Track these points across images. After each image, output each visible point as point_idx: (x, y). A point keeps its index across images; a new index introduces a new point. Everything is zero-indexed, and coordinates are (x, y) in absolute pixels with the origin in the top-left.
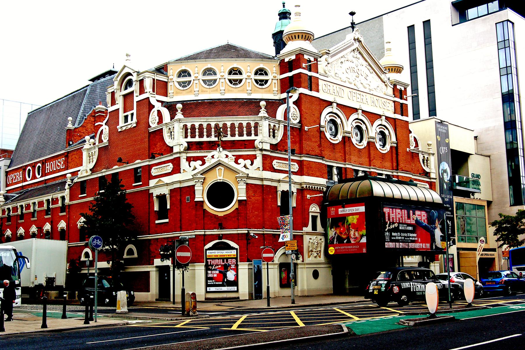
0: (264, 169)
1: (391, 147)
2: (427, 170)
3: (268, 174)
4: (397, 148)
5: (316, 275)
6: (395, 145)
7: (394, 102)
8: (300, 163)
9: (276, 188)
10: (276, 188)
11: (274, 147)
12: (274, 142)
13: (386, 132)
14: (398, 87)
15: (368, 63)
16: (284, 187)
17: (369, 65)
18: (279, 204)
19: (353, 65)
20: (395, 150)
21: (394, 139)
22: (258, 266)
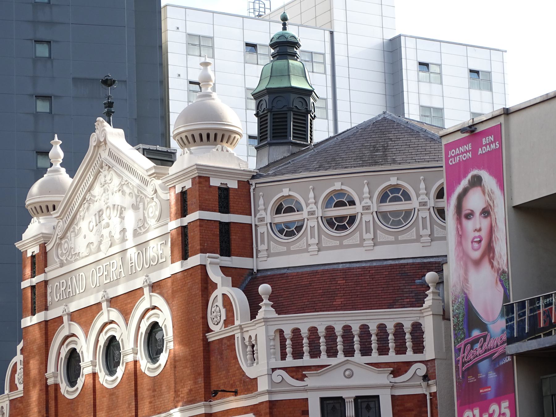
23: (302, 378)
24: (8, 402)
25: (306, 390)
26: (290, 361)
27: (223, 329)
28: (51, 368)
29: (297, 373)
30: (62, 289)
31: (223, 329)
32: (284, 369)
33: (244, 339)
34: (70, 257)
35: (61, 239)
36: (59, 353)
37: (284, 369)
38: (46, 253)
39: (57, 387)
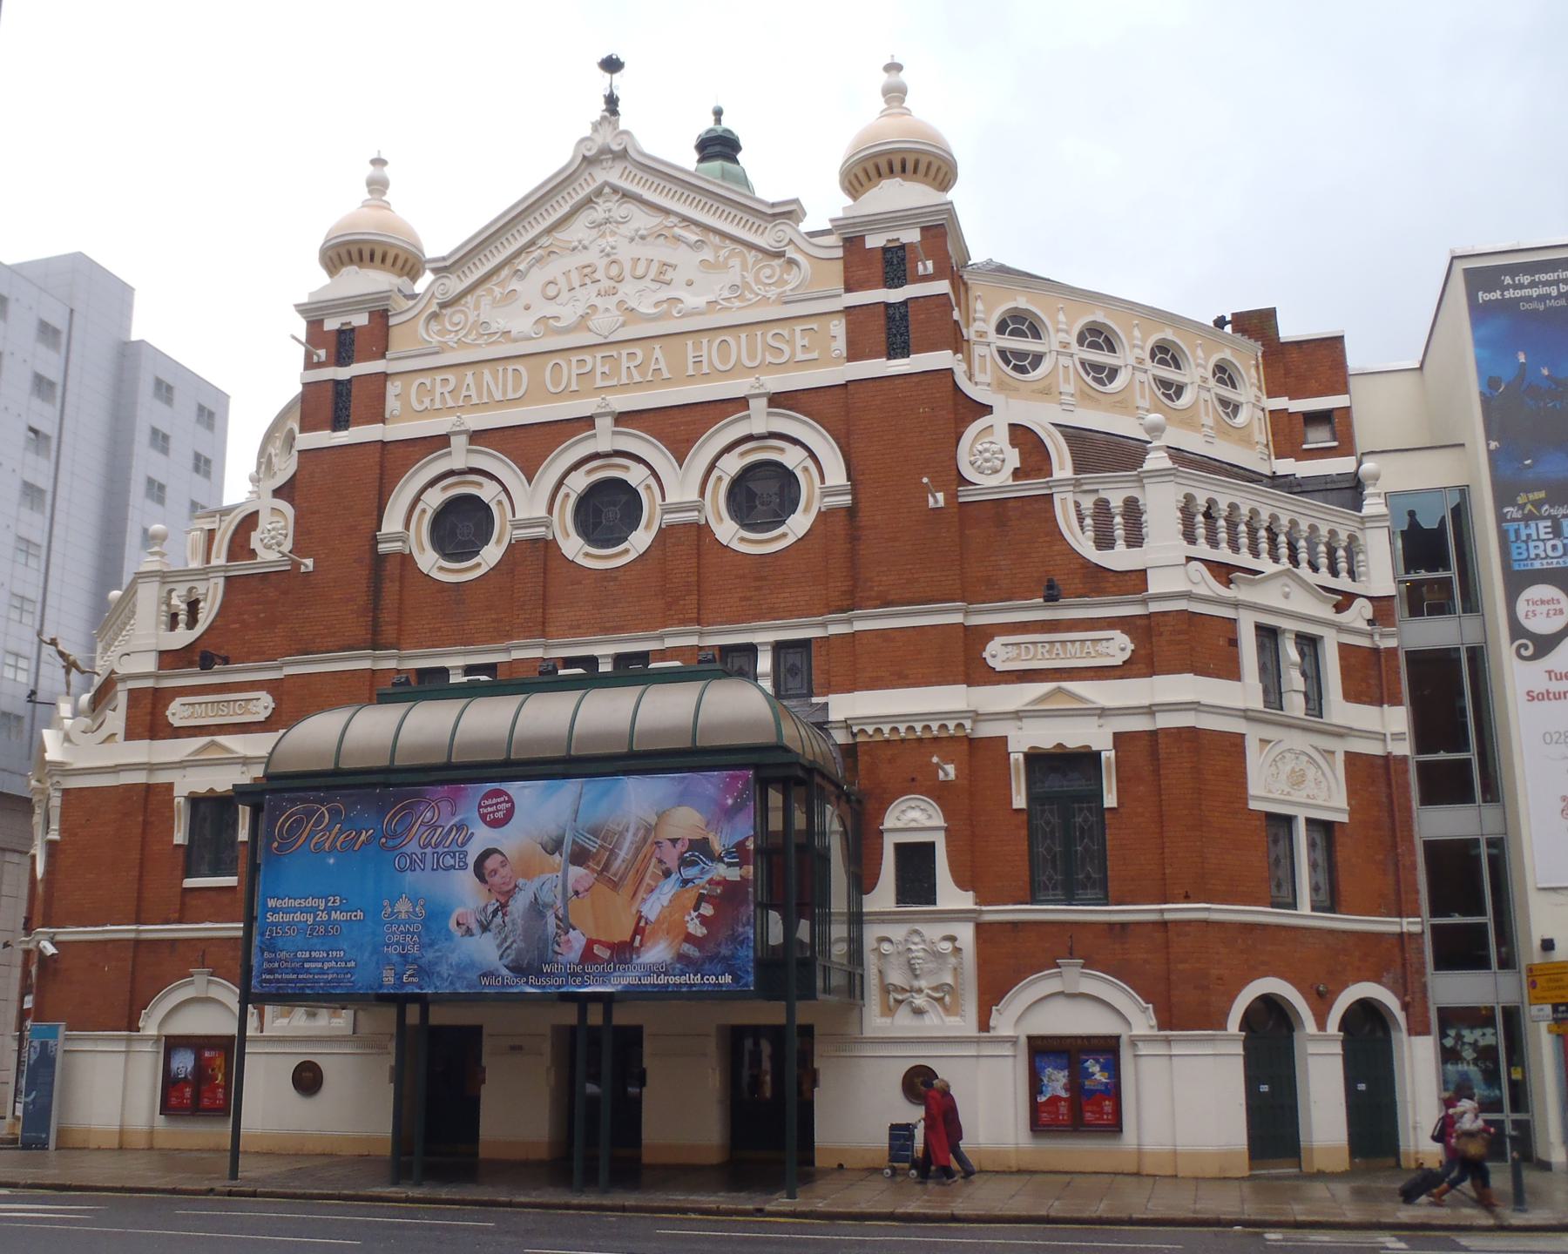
0: (130, 735)
1: (824, 516)
2: (1119, 558)
3: (143, 751)
4: (851, 512)
5: (307, 1079)
6: (846, 500)
7: (848, 310)
8: (272, 687)
9: (170, 786)
10: (170, 786)
11: (170, 659)
12: (182, 637)
13: (792, 458)
14: (874, 241)
15: (677, 214)
16: (187, 784)
17: (685, 219)
18: (180, 837)
19: (592, 256)
20: (843, 525)
21: (836, 474)
22: (44, 1045)
23: (1228, 583)
24: (221, 582)
25: (1236, 605)
26: (1203, 549)
27: (1010, 482)
28: (392, 523)
29: (1223, 572)
30: (438, 390)
31: (1010, 482)
32: (1207, 562)
33: (1077, 505)
34: (473, 336)
35: (443, 306)
36: (417, 500)
37: (1207, 562)
38: (387, 328)
39: (406, 560)
